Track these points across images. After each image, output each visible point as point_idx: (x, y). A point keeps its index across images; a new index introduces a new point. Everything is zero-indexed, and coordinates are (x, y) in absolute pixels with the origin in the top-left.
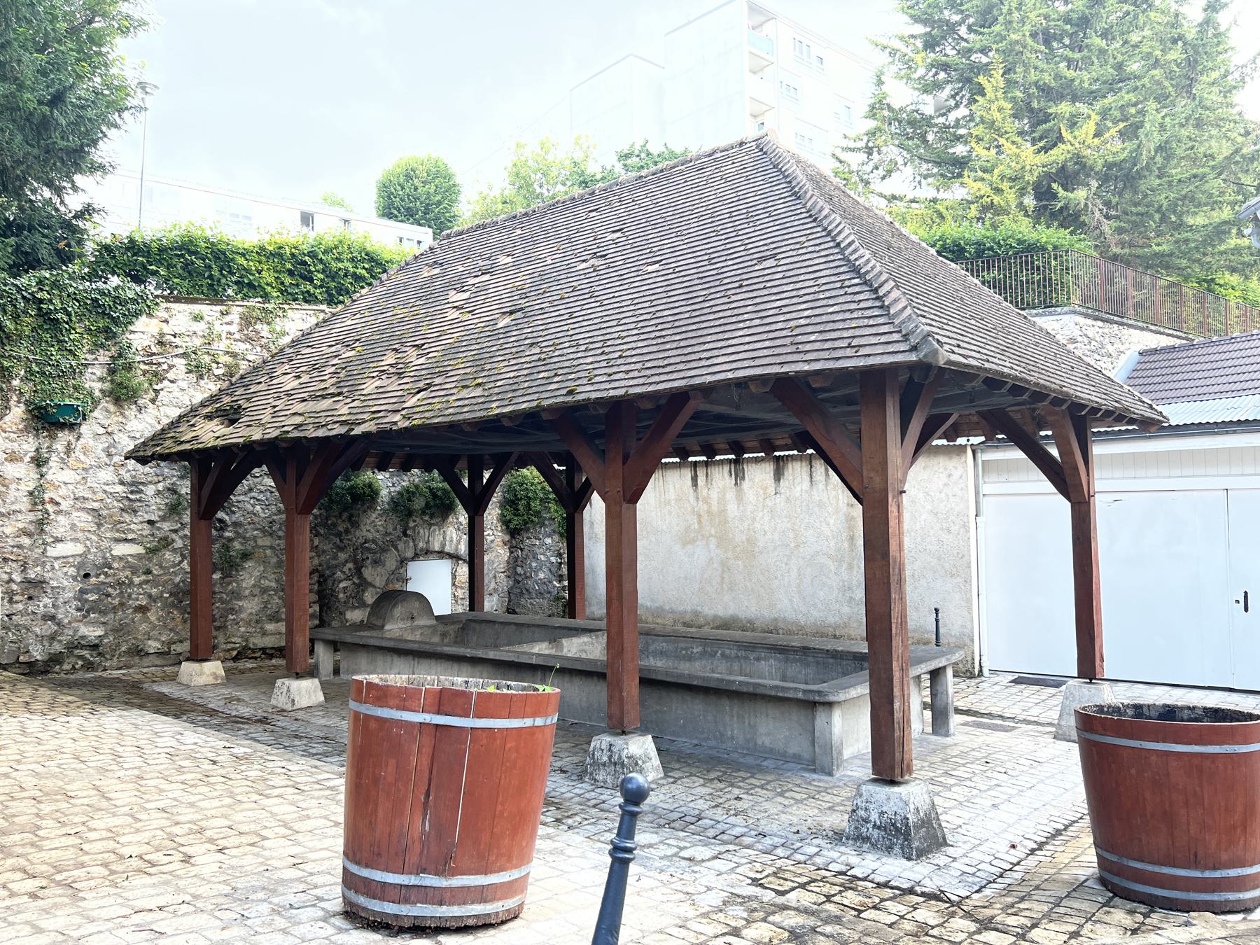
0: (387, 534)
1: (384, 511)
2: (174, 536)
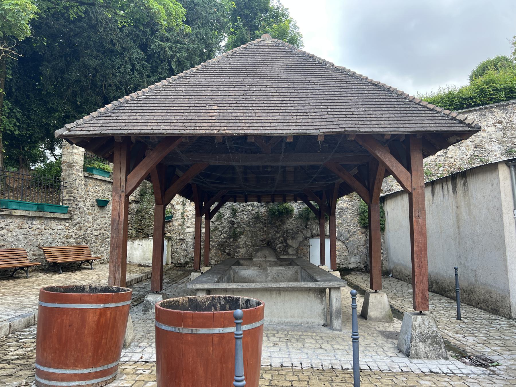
0: (297, 227)
1: (296, 218)
2: (219, 226)
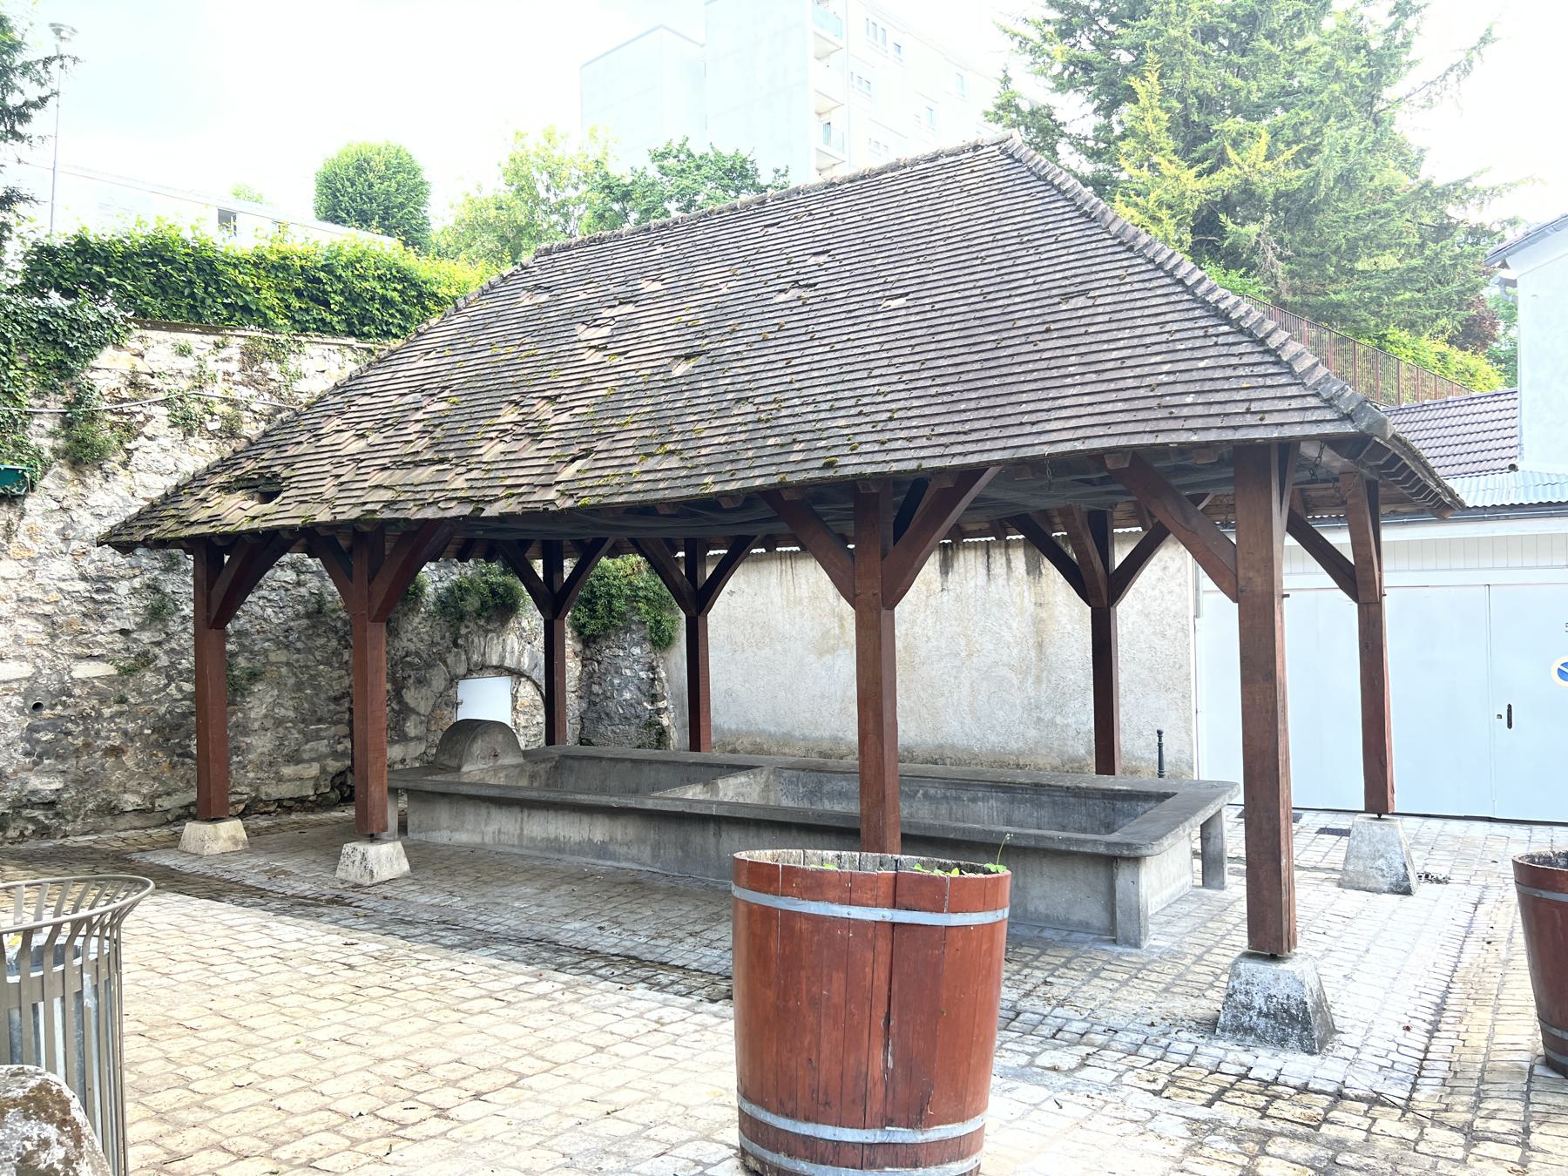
0: (433, 644)
2: (157, 650)
